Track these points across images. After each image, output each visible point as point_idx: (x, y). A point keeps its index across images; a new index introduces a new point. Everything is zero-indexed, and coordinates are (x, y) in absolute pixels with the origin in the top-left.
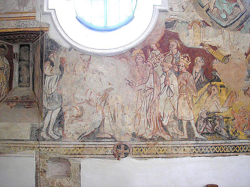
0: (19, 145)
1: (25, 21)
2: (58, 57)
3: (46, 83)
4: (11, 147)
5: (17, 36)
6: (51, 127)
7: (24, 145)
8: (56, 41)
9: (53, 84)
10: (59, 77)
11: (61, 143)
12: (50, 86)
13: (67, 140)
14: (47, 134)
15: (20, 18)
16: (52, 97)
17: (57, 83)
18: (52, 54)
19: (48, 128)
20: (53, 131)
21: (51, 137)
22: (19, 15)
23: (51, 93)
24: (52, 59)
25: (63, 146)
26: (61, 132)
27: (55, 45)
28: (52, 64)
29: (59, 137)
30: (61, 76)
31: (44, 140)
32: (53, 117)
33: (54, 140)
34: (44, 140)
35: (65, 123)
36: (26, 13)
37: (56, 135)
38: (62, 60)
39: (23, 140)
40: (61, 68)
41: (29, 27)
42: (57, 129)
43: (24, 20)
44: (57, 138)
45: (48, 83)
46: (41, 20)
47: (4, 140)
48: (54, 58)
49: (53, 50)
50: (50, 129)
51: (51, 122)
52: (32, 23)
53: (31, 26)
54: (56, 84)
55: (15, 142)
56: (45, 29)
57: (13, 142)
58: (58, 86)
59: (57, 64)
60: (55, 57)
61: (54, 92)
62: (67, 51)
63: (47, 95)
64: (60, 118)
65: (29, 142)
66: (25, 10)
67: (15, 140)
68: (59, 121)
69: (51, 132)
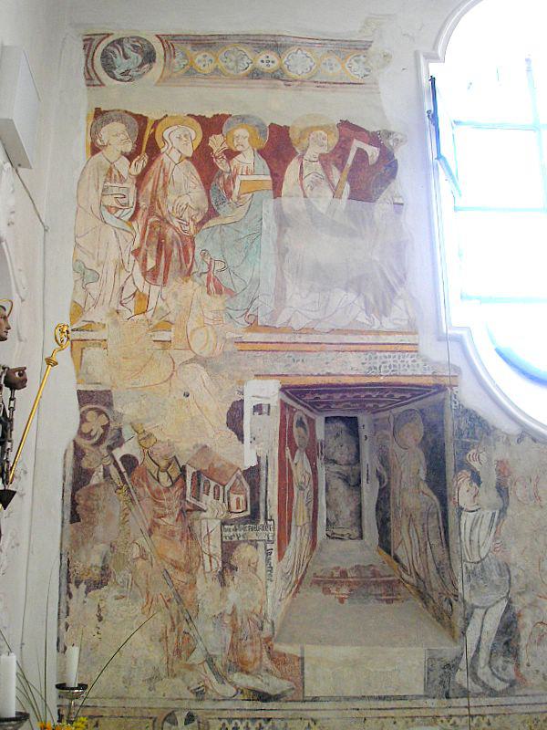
0: (391, 713)
1: (390, 357)
2: (489, 459)
3: (463, 531)
4: (368, 721)
5: (337, 397)
6: (484, 655)
7: (408, 713)
8: (480, 414)
9: (483, 533)
10: (497, 515)
11: (513, 700)
12: (475, 538)
13: (529, 692)
14: (473, 673)
15: (374, 348)
16: (483, 570)
17: (493, 530)
18: (474, 451)
19: (475, 658)
20: (490, 667)
21: (484, 685)
22: (371, 339)
23: (477, 559)
24: (475, 465)
25: (520, 709)
26: (511, 667)
27: (477, 427)
28: (476, 478)
29: (508, 685)
30: (503, 511)
31: (466, 693)
32: (487, 627)
33: (493, 693)
34: (466, 693)
35: (523, 643)
36: (389, 333)
37: (499, 678)
38: (503, 469)
39: (404, 698)
40: (502, 490)
41: (402, 373)
42: (500, 662)
43: (387, 354)
44: (500, 686)
45: (468, 531)
46: (433, 352)
47: (347, 699)
48: (480, 460)
49: (476, 438)
50: (482, 663)
51: (483, 642)
52: (410, 363)
53: (408, 370)
54: (492, 535)
55: (381, 704)
56: (446, 381)
57: (373, 704)
58: (495, 539)
59: (490, 478)
60: (483, 457)
61: (487, 555)
62: (513, 443)
63: (469, 565)
64: (508, 629)
65: (422, 702)
66: (388, 325)
67: (380, 698)
68: (506, 639)
69: (483, 671)
